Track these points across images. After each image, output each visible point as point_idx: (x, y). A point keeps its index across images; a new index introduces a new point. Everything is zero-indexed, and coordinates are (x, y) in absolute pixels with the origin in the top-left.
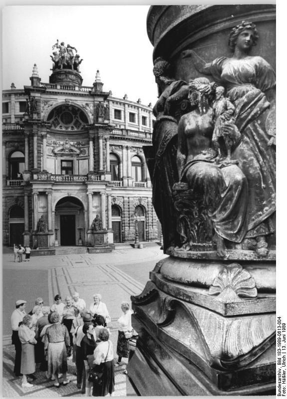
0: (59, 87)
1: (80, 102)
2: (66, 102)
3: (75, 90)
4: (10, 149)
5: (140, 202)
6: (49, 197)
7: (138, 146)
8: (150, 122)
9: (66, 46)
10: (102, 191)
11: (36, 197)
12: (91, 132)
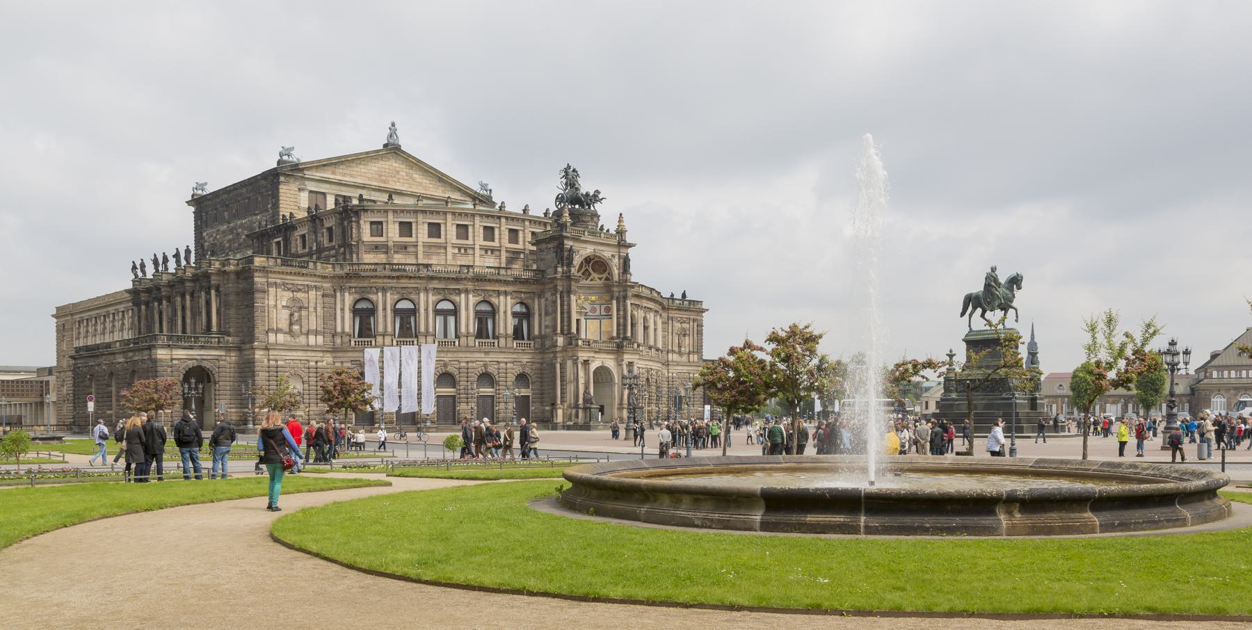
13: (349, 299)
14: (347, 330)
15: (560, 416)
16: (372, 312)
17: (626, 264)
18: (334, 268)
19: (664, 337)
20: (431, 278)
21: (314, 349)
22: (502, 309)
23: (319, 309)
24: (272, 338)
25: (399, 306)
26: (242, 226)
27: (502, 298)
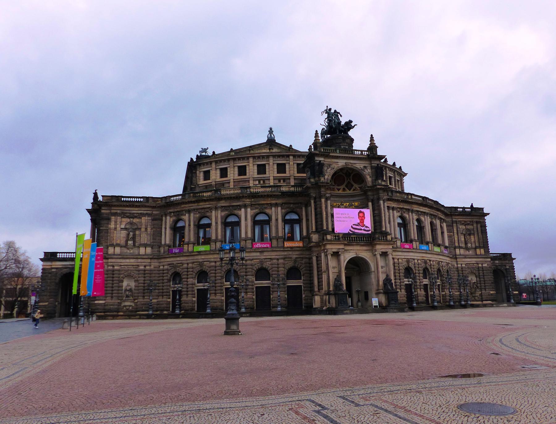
0: (338, 151)
2: (346, 165)
3: (352, 153)
4: (286, 210)
5: (408, 264)
6: (342, 257)
7: (401, 207)
8: (395, 182)
9: (333, 111)
10: (390, 251)
11: (329, 257)
12: (369, 193)
13: (169, 221)
15: (317, 302)
18: (161, 201)
19: (449, 237)
20: (219, 199)
21: (142, 257)
23: (149, 229)
24: (111, 250)
27: (273, 208)
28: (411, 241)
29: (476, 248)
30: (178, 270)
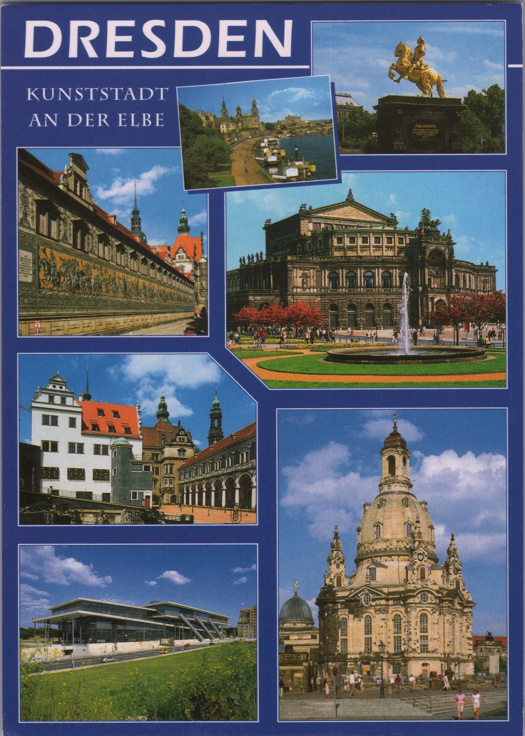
1: (443, 248)
13: (327, 273)
14: (327, 285)
16: (338, 278)
17: (452, 252)
22: (394, 275)
23: (314, 277)
24: (295, 290)
25: (349, 275)
26: (285, 238)
27: (394, 270)
28: (460, 289)
29: (489, 292)
30: (335, 303)
